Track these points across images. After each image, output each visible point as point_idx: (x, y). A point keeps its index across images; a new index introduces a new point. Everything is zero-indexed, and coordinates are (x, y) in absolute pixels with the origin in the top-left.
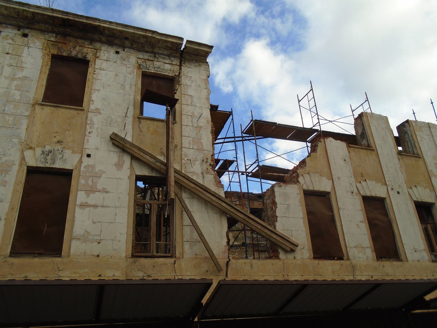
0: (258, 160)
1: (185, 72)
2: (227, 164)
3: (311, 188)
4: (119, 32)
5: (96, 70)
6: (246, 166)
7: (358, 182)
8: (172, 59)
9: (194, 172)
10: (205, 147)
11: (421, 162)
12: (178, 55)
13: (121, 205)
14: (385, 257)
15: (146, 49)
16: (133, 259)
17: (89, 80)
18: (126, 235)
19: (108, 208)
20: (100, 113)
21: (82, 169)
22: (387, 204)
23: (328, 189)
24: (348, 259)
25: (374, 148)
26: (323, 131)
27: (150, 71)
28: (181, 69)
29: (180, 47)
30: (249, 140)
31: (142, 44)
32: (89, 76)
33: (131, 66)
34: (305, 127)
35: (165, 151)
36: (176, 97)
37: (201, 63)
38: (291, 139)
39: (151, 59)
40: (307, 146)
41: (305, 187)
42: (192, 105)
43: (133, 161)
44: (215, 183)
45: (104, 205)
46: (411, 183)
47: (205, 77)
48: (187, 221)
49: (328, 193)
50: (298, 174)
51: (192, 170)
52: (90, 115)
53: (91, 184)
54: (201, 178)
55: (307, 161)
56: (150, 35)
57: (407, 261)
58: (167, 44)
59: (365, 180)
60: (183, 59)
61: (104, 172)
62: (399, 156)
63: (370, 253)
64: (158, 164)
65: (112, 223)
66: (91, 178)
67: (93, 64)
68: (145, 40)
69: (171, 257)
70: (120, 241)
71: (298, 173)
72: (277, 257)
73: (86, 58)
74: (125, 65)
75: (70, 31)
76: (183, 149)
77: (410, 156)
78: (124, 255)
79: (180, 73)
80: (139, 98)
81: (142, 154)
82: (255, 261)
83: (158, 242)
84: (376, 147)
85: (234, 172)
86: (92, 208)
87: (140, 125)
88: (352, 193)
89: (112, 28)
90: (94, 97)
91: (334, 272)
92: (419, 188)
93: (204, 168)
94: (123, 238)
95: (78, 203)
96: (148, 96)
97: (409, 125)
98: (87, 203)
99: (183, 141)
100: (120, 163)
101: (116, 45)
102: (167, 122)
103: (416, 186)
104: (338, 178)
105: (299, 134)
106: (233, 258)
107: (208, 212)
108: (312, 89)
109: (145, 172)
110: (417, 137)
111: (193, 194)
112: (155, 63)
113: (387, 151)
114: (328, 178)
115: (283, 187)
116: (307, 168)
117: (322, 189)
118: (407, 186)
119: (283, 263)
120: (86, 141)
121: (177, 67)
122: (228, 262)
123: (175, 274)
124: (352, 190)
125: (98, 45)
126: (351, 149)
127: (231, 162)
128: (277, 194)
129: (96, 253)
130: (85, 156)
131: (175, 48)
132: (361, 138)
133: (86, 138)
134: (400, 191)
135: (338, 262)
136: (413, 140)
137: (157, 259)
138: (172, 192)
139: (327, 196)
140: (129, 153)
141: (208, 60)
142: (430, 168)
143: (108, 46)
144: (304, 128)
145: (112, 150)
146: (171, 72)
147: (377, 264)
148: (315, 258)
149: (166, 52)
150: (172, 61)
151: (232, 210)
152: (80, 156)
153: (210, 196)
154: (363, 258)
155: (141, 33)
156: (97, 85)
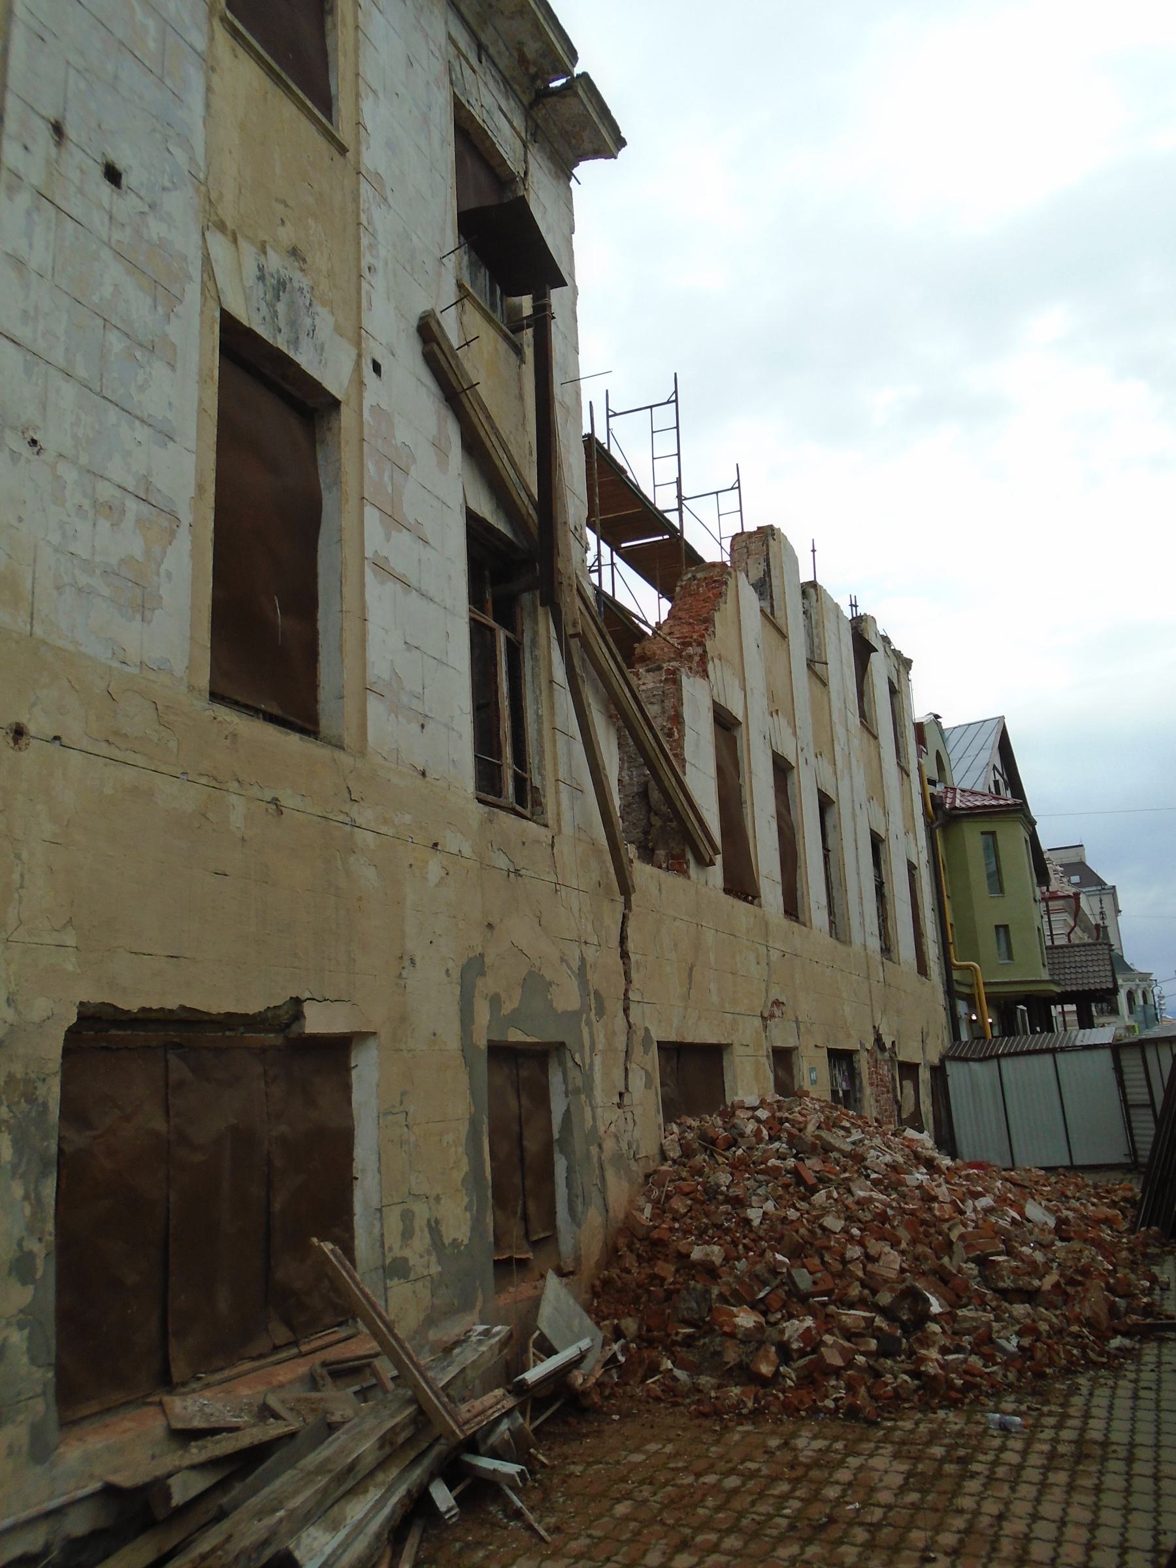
24: (760, 906)
50: (705, 651)
72: (685, 873)
131: (533, 70)
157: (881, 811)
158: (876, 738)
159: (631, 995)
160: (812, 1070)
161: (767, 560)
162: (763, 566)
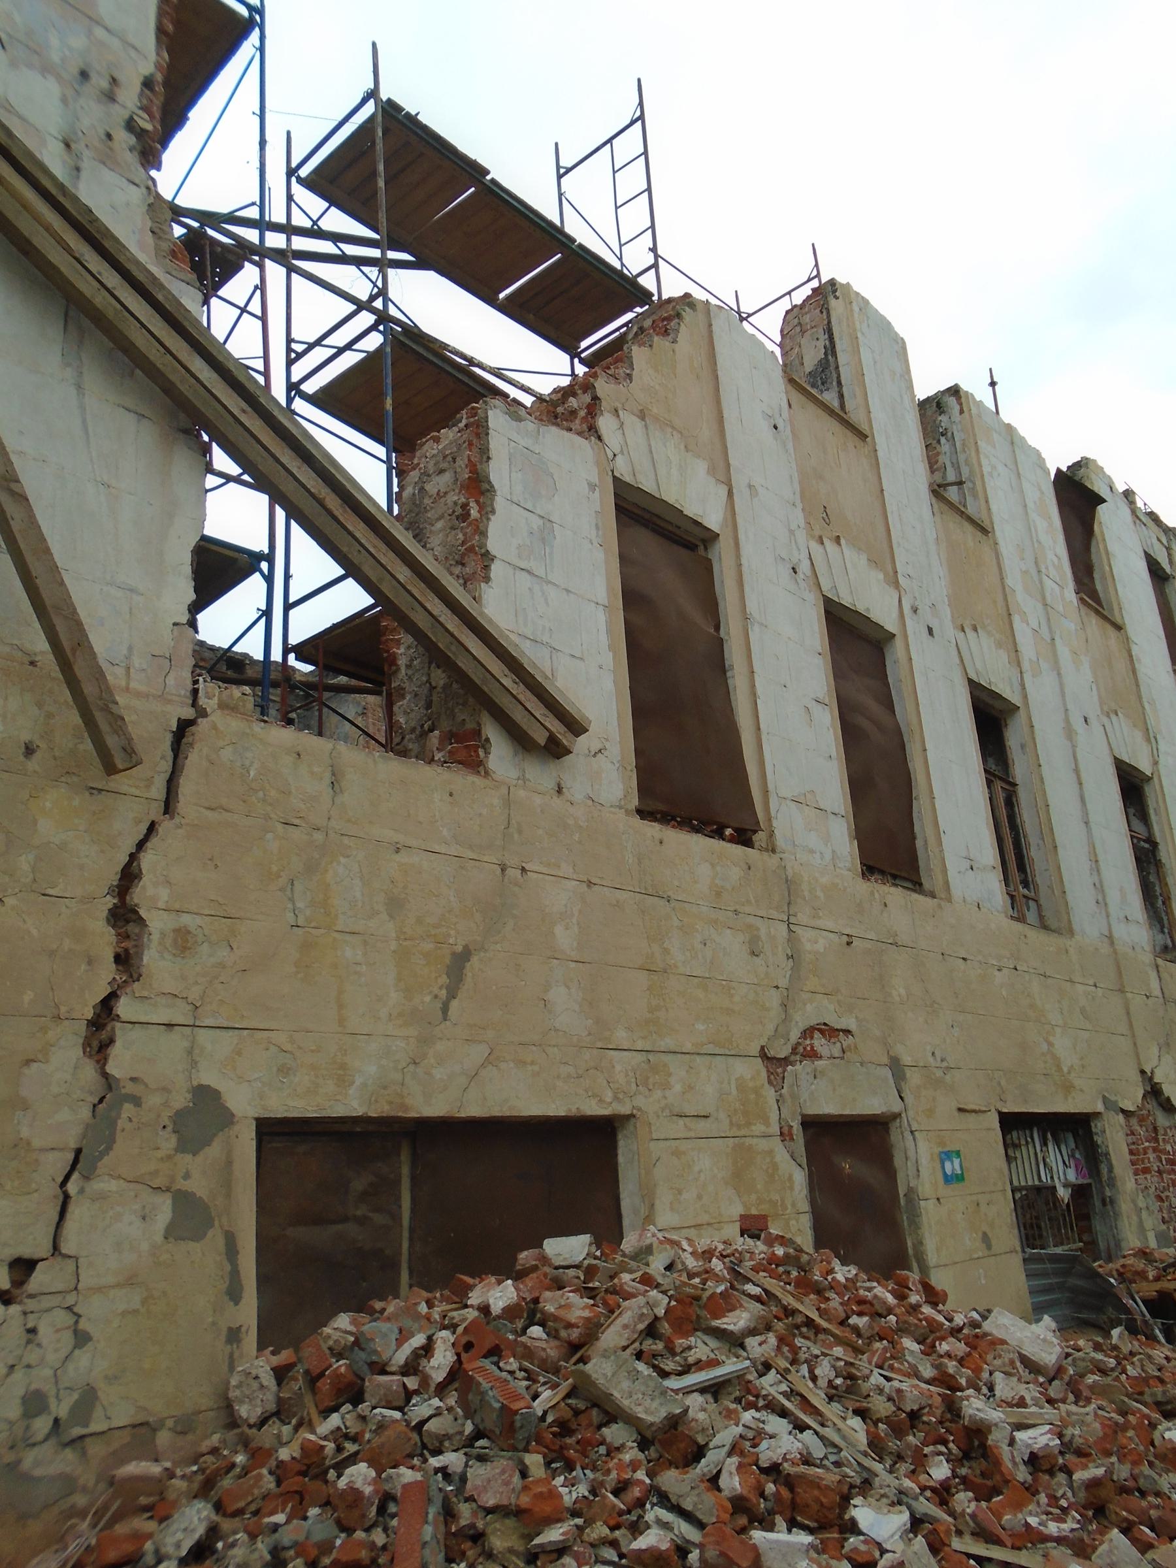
3: (648, 486)
7: (813, 537)
14: (882, 872)
23: (713, 520)
41: (623, 469)
50: (595, 398)
57: (949, 900)
71: (600, 394)
91: (718, 894)
97: (961, 404)
104: (750, 486)
107: (79, 387)
108: (641, 118)
114: (712, 471)
119: (508, 803)
122: (184, 726)
124: (795, 560)
135: (737, 850)
136: (967, 462)
142: (1009, 582)
147: (863, 888)
148: (642, 813)
153: (112, 279)
157: (1138, 735)
158: (1119, 628)
159: (124, 1008)
160: (947, 1155)
161: (829, 331)
162: (823, 339)
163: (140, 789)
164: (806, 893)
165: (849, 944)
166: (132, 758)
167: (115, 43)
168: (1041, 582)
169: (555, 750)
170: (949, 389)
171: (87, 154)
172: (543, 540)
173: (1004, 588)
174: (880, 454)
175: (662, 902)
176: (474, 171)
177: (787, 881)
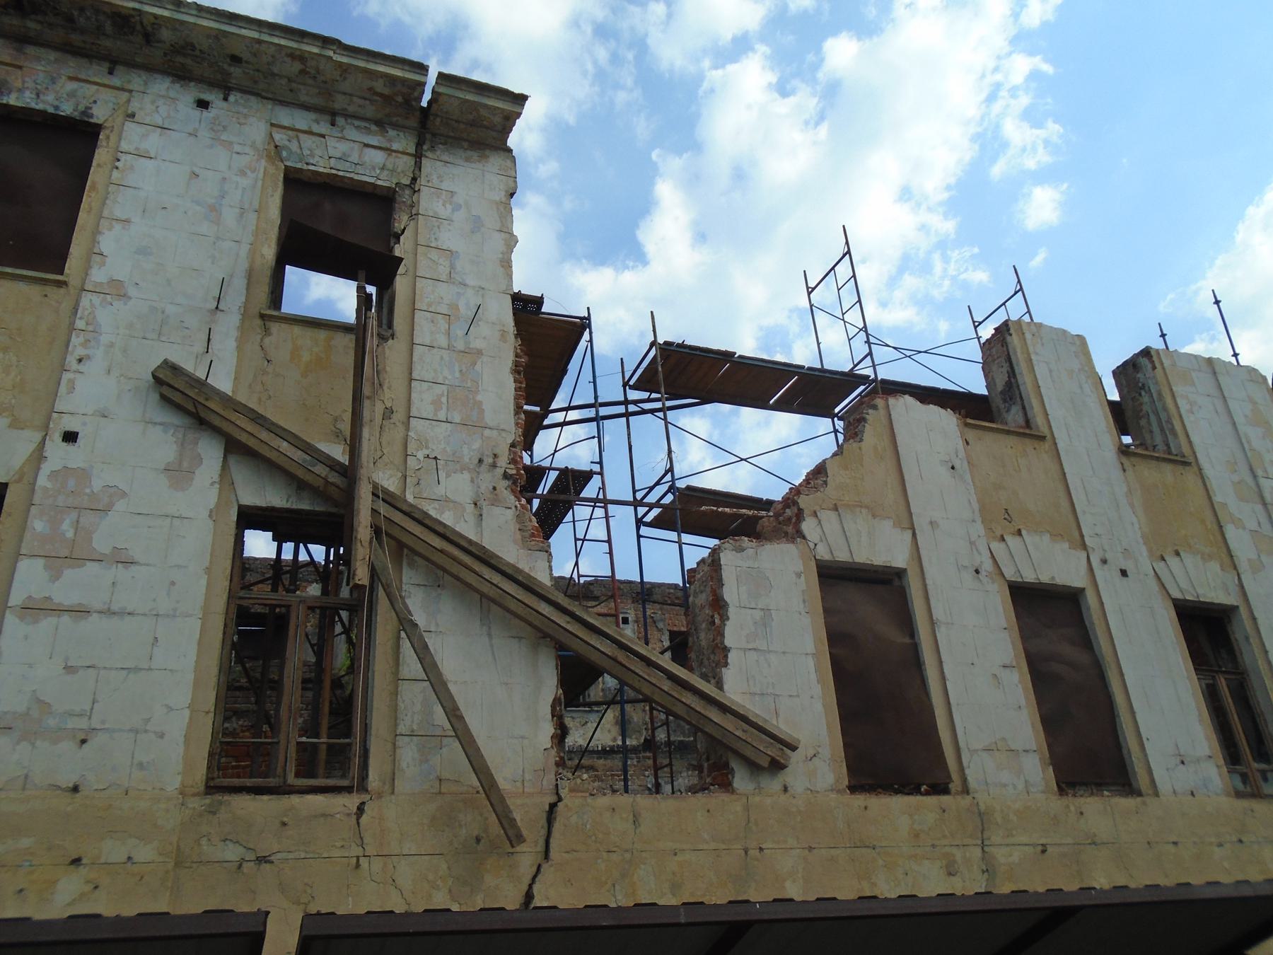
0: (670, 470)
1: (435, 181)
2: (573, 481)
3: (842, 556)
4: (208, 37)
5: (123, 157)
6: (635, 491)
7: (994, 538)
8: (392, 133)
9: (447, 500)
10: (489, 419)
11: (1190, 477)
12: (413, 122)
13: (175, 610)
14: (1085, 784)
15: (303, 98)
16: (207, 801)
17: (93, 188)
18: (187, 713)
19: (128, 618)
20: (124, 296)
21: (42, 481)
22: (1088, 609)
23: (899, 559)
24: (966, 790)
25: (1044, 430)
26: (883, 381)
27: (311, 168)
28: (418, 166)
29: (416, 94)
30: (652, 411)
31: (290, 80)
32: (96, 175)
33: (247, 150)
34: (826, 367)
35: (346, 427)
36: (398, 252)
37: (487, 152)
38: (784, 406)
39: (316, 128)
40: (836, 431)
41: (823, 553)
42: (450, 280)
43: (232, 460)
44: (519, 536)
45: (115, 607)
46: (1164, 546)
47: (499, 195)
48: (411, 665)
49: (900, 573)
50: (800, 511)
51: (440, 491)
52: (86, 300)
53: (70, 534)
54: (471, 519)
55: (830, 470)
56: (315, 50)
57: (1156, 794)
58: (374, 84)
59: (1019, 533)
60: (428, 136)
61: (124, 494)
62: (1124, 460)
63: (1035, 771)
64: (321, 470)
65: (137, 670)
66: (74, 515)
67: (113, 138)
68: (297, 66)
69: (349, 790)
70: (162, 735)
71: (802, 506)
72: (726, 786)
73: (92, 116)
74: (228, 145)
75: (38, 27)
76: (413, 422)
77: (1157, 459)
78: (173, 784)
79: (414, 179)
80: (269, 252)
81: (264, 435)
82: (644, 801)
83: (304, 739)
84: (1050, 427)
85: (594, 502)
86: (66, 618)
87: (267, 340)
88: (977, 572)
89: (182, 23)
90: (107, 243)
91: (917, 836)
92: (1188, 559)
93: (483, 489)
94: (177, 726)
95: (16, 598)
96: (304, 245)
98: (48, 599)
99: (413, 395)
100: (185, 464)
101: (200, 80)
102: (357, 331)
103: (1178, 554)
105: (811, 391)
106: (571, 790)
107: (489, 635)
108: (849, 252)
109: (275, 497)
110: (1179, 400)
111: (440, 573)
112: (331, 142)
113: (1086, 442)
114: (897, 524)
115: (750, 552)
116: (831, 491)
117: (879, 560)
118: (1150, 551)
119: (747, 808)
120: (63, 389)
121: (405, 158)
122: (553, 806)
123: (359, 852)
125: (136, 80)
126: (971, 435)
127: (585, 477)
128: (728, 574)
129: (67, 780)
130: (57, 436)
131: (400, 99)
132: (1005, 401)
133: (66, 376)
134: (1129, 566)
136: (1165, 409)
137: (295, 800)
138: (358, 564)
139: (896, 582)
140: (217, 431)
141: (512, 141)
142: (1218, 498)
143: (173, 82)
144: (822, 370)
145: (159, 420)
146: (386, 173)
147: (1057, 804)
148: (853, 789)
149: (370, 111)
150: (390, 141)
151: (574, 627)
152: (38, 437)
153: (497, 578)
154: (1015, 787)
155: (283, 42)
156: (122, 205)
161: (1009, 360)
163: (527, 857)
164: (999, 820)
165: (1044, 851)
166: (520, 838)
167: (495, 432)
168: (1258, 485)
169: (777, 766)
170: (1142, 351)
171: (484, 504)
172: (765, 625)
173: (1212, 505)
174: (1061, 445)
175: (869, 850)
176: (728, 356)
177: (980, 814)
